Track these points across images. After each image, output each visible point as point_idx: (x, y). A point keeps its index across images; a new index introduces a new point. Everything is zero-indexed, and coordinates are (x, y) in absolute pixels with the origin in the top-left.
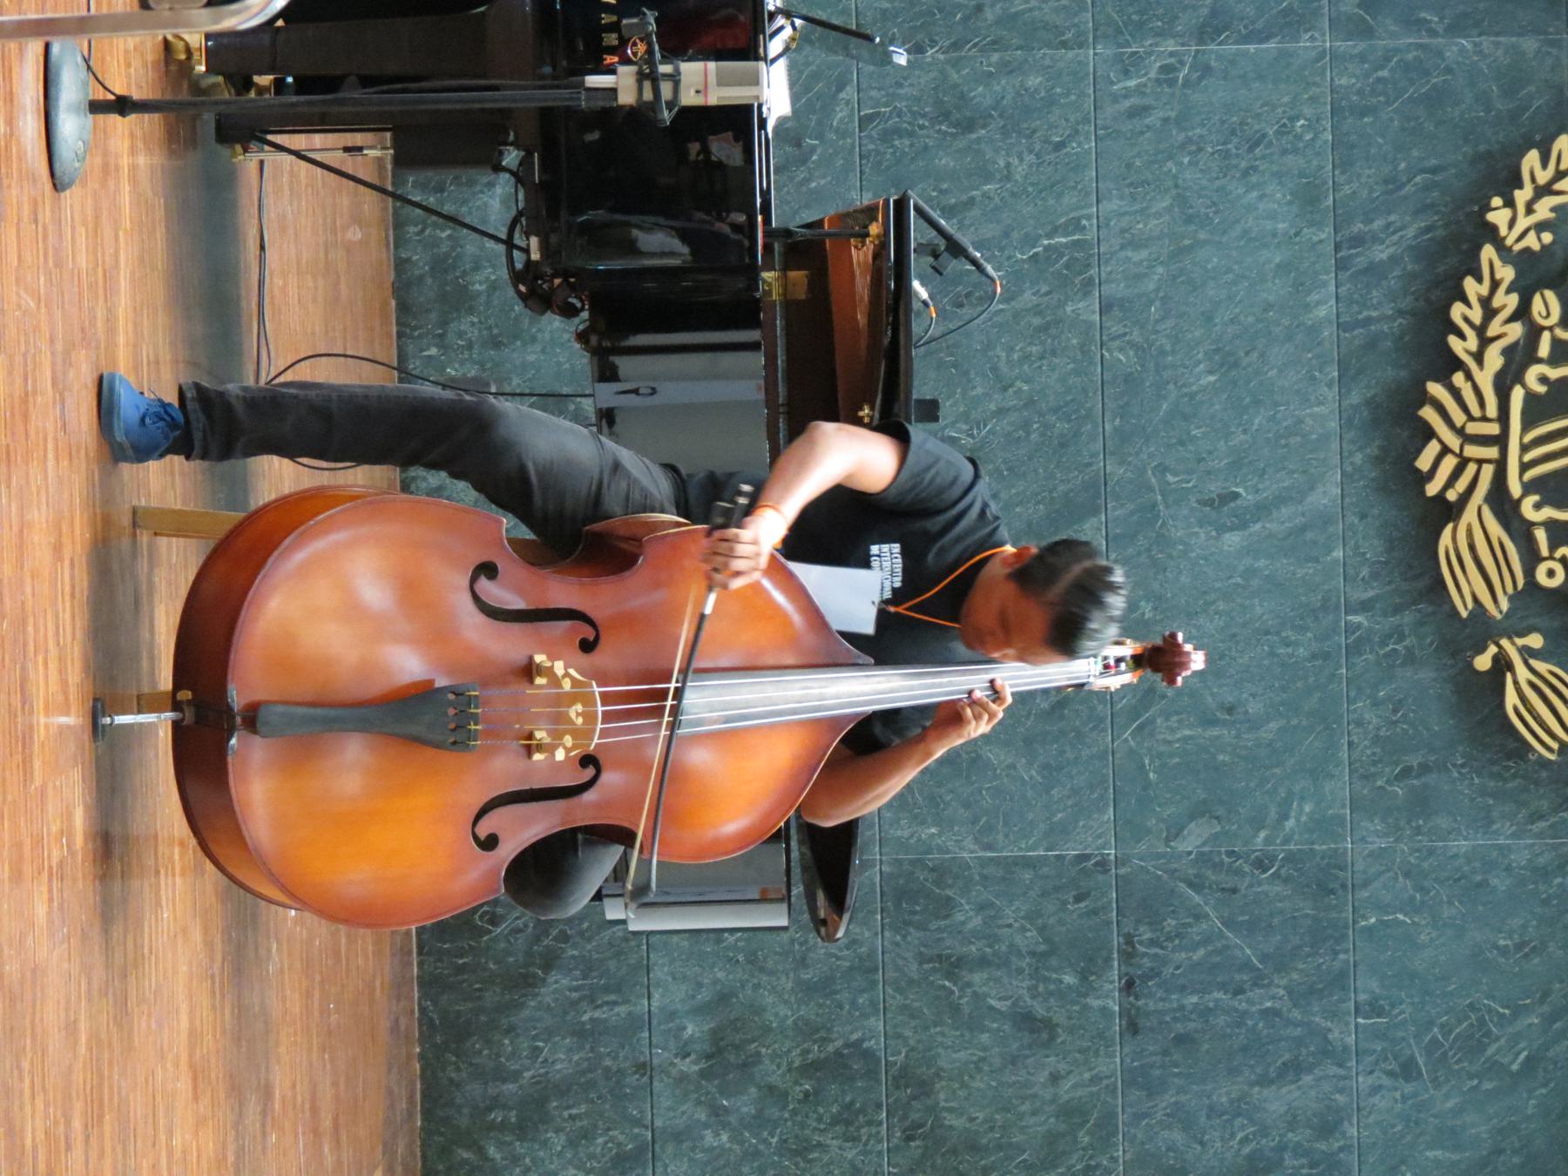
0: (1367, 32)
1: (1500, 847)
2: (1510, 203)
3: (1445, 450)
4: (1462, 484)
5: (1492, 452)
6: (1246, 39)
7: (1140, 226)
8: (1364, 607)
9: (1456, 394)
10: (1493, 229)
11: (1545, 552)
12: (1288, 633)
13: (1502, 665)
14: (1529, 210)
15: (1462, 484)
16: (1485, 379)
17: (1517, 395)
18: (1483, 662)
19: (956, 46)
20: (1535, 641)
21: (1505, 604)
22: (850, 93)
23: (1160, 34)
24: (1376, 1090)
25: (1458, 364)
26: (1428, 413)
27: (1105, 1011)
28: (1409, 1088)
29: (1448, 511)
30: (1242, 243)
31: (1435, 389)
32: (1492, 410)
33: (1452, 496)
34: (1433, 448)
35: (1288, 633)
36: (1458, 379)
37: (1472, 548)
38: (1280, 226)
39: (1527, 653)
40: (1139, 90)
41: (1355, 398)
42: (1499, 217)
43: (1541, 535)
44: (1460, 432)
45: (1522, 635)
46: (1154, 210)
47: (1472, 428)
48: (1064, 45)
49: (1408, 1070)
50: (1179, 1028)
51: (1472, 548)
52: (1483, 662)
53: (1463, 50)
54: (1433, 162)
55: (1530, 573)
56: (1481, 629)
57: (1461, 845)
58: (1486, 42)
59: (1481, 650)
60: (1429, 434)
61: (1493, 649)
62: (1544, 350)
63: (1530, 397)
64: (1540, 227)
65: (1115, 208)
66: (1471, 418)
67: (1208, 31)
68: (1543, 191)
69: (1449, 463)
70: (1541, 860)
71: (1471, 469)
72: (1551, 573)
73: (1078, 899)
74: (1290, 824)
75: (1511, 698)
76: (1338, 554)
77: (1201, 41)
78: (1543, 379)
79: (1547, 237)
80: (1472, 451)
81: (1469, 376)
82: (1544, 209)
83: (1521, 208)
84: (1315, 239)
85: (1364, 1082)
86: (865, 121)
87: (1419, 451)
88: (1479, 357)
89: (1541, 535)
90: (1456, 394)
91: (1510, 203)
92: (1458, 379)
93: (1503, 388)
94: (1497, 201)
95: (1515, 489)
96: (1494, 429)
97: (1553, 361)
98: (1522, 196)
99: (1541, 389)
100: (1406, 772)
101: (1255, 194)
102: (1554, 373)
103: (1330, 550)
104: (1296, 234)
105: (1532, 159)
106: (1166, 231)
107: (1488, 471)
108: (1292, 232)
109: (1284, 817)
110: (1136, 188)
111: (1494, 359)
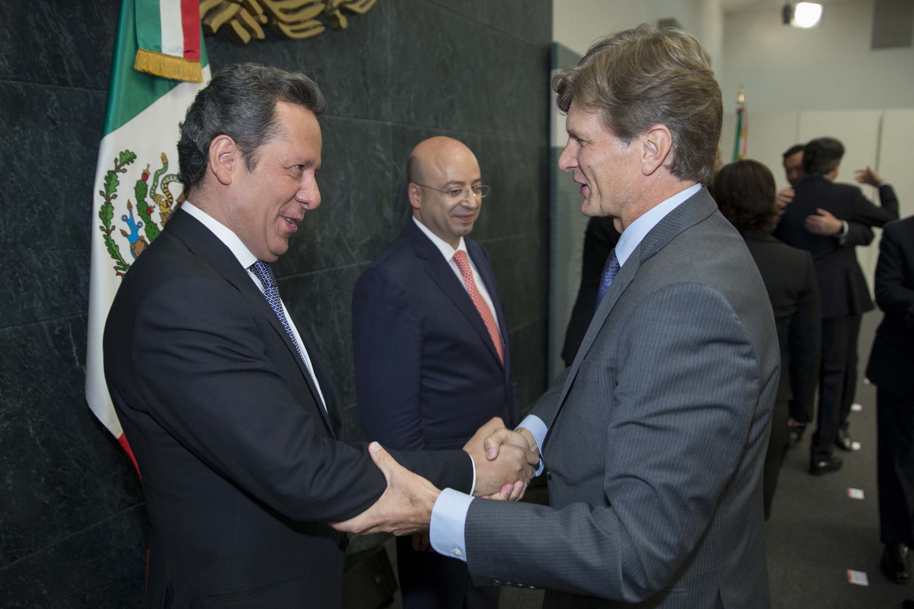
3: (236, 17)
4: (259, 10)
7: (56, 277)
15: (259, 10)
30: (66, 178)
34: (235, 25)
38: (47, 138)
46: (41, 265)
52: (343, 22)
60: (226, 27)
61: (338, 13)
65: (40, 304)
84: (57, 105)
101: (16, 162)
104: (55, 124)
106: (59, 252)
108: (52, 127)
110: (19, 285)
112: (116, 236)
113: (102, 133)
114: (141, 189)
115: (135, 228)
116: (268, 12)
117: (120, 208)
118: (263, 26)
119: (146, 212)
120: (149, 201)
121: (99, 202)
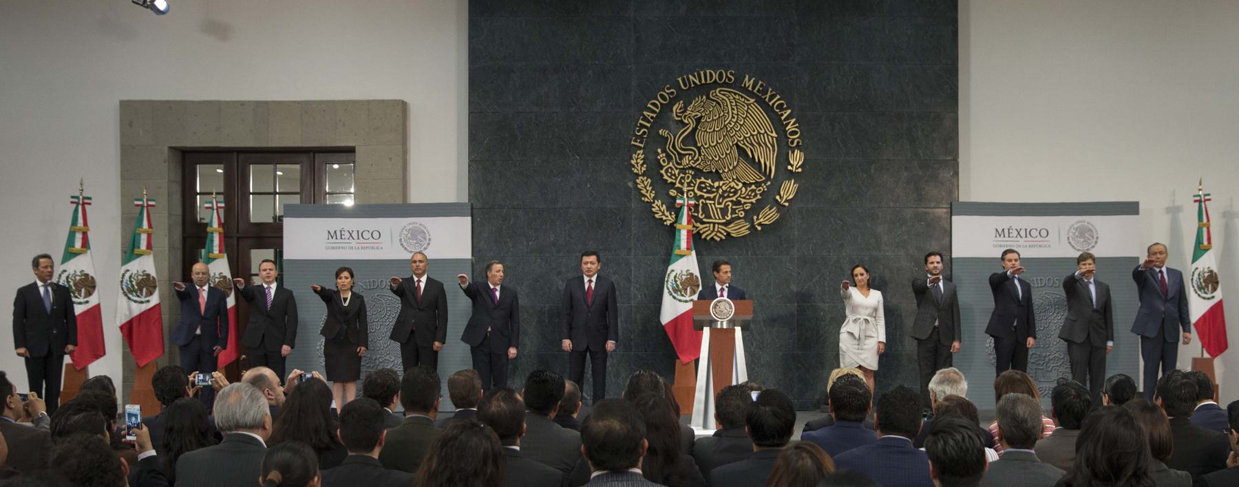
0: (630, 248)
1: (797, 225)
2: (666, 220)
3: (716, 235)
4: (723, 232)
5: (716, 225)
6: (631, 271)
8: (747, 252)
9: (704, 232)
10: (671, 224)
11: (736, 215)
12: (753, 267)
13: (760, 224)
14: (667, 216)
15: (723, 232)
16: (701, 226)
17: (705, 220)
18: (759, 228)
19: (631, 332)
20: (755, 217)
21: (747, 224)
22: (640, 354)
23: (629, 289)
24: (846, 252)
25: (698, 232)
26: (708, 238)
27: (828, 306)
28: (846, 245)
29: (728, 234)
31: (703, 236)
32: (708, 225)
33: (725, 234)
34: (715, 237)
35: (753, 267)
36: (701, 232)
37: (736, 230)
39: (757, 219)
40: (641, 295)
41: (705, 253)
42: (668, 223)
43: (733, 216)
44: (712, 232)
45: (753, 220)
47: (711, 229)
48: (631, 310)
49: (842, 245)
50: (832, 291)
51: (736, 230)
52: (759, 228)
53: (635, 229)
54: (657, 236)
55: (740, 218)
56: (753, 228)
57: (796, 233)
58: (633, 224)
59: (756, 228)
60: (712, 238)
62: (696, 214)
63: (706, 217)
64: (671, 214)
66: (709, 230)
67: (630, 282)
68: (663, 214)
69: (718, 234)
70: (800, 217)
71: (720, 230)
72: (741, 214)
73: (805, 311)
74: (791, 268)
75: (767, 223)
76: (736, 257)
77: (630, 282)
78: (702, 215)
79: (673, 213)
80: (716, 230)
81: (701, 230)
82: (668, 214)
83: (667, 218)
85: (844, 254)
86: (646, 351)
87: (716, 241)
88: (697, 228)
89: (733, 216)
90: (704, 232)
91: (666, 220)
92: (701, 232)
93: (703, 223)
94: (665, 223)
95: (724, 221)
96: (712, 225)
97: (698, 213)
98: (664, 218)
99: (704, 215)
100: (781, 244)
102: (701, 213)
103: (735, 259)
105: (657, 216)
107: (720, 226)
109: (790, 269)
111: (698, 225)
112: (669, 286)
113: (669, 265)
114: (675, 277)
115: (673, 284)
116: (726, 231)
117: (670, 280)
118: (725, 236)
119: (676, 281)
120: (677, 279)
121: (666, 279)
